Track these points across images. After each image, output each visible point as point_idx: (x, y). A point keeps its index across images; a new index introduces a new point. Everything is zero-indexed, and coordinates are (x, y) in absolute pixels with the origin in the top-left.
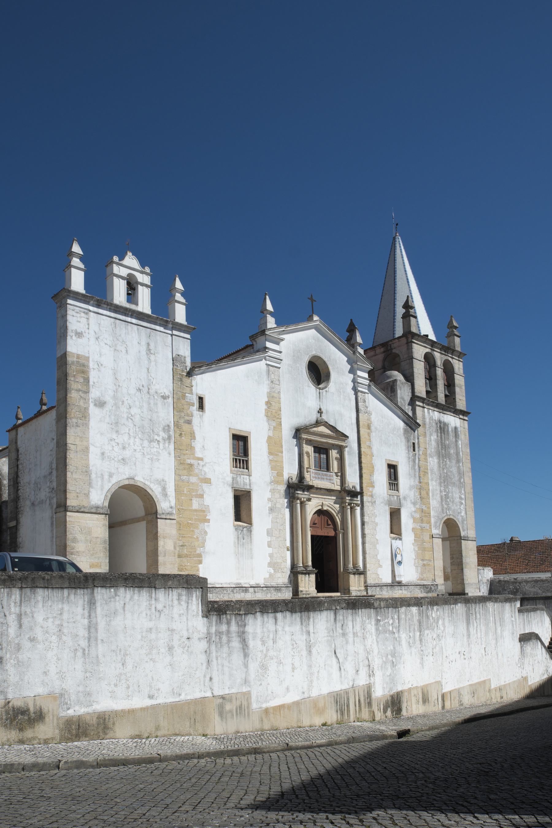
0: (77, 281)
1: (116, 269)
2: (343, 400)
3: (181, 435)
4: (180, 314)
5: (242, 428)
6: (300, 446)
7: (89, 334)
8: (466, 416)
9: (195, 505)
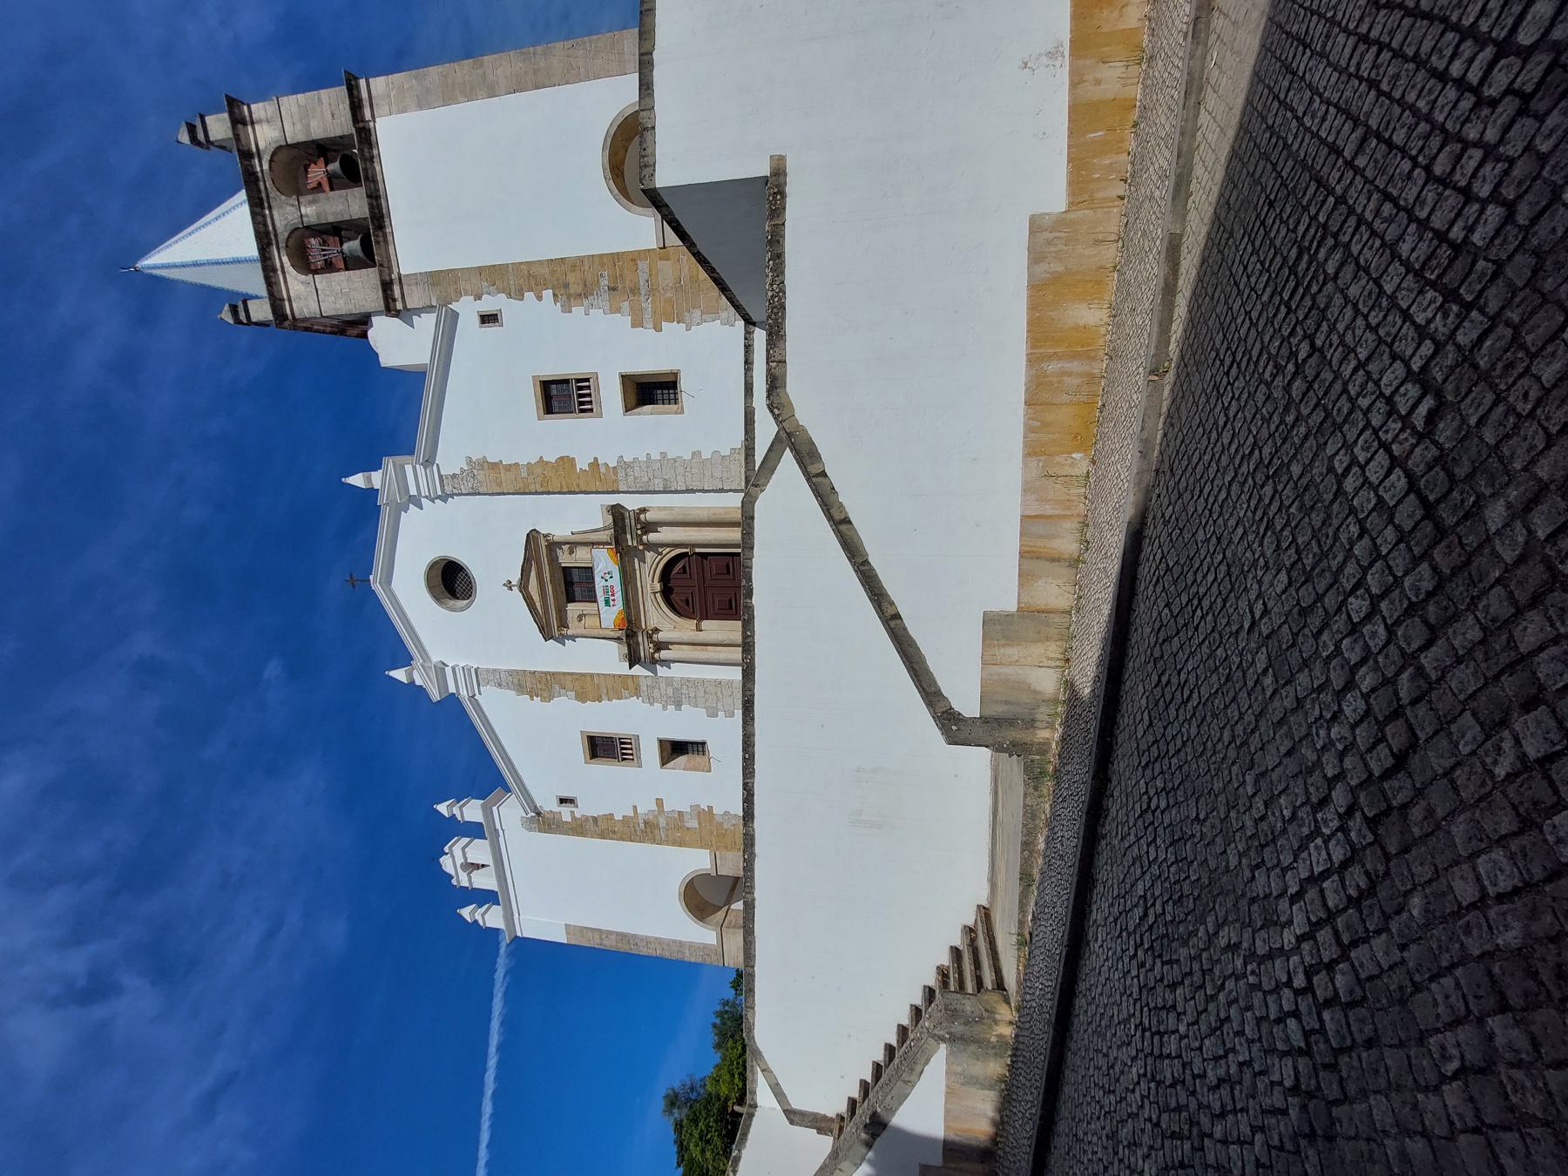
1: (465, 883)
3: (614, 832)
4: (472, 811)
6: (573, 638)
8: (358, 87)
9: (693, 824)
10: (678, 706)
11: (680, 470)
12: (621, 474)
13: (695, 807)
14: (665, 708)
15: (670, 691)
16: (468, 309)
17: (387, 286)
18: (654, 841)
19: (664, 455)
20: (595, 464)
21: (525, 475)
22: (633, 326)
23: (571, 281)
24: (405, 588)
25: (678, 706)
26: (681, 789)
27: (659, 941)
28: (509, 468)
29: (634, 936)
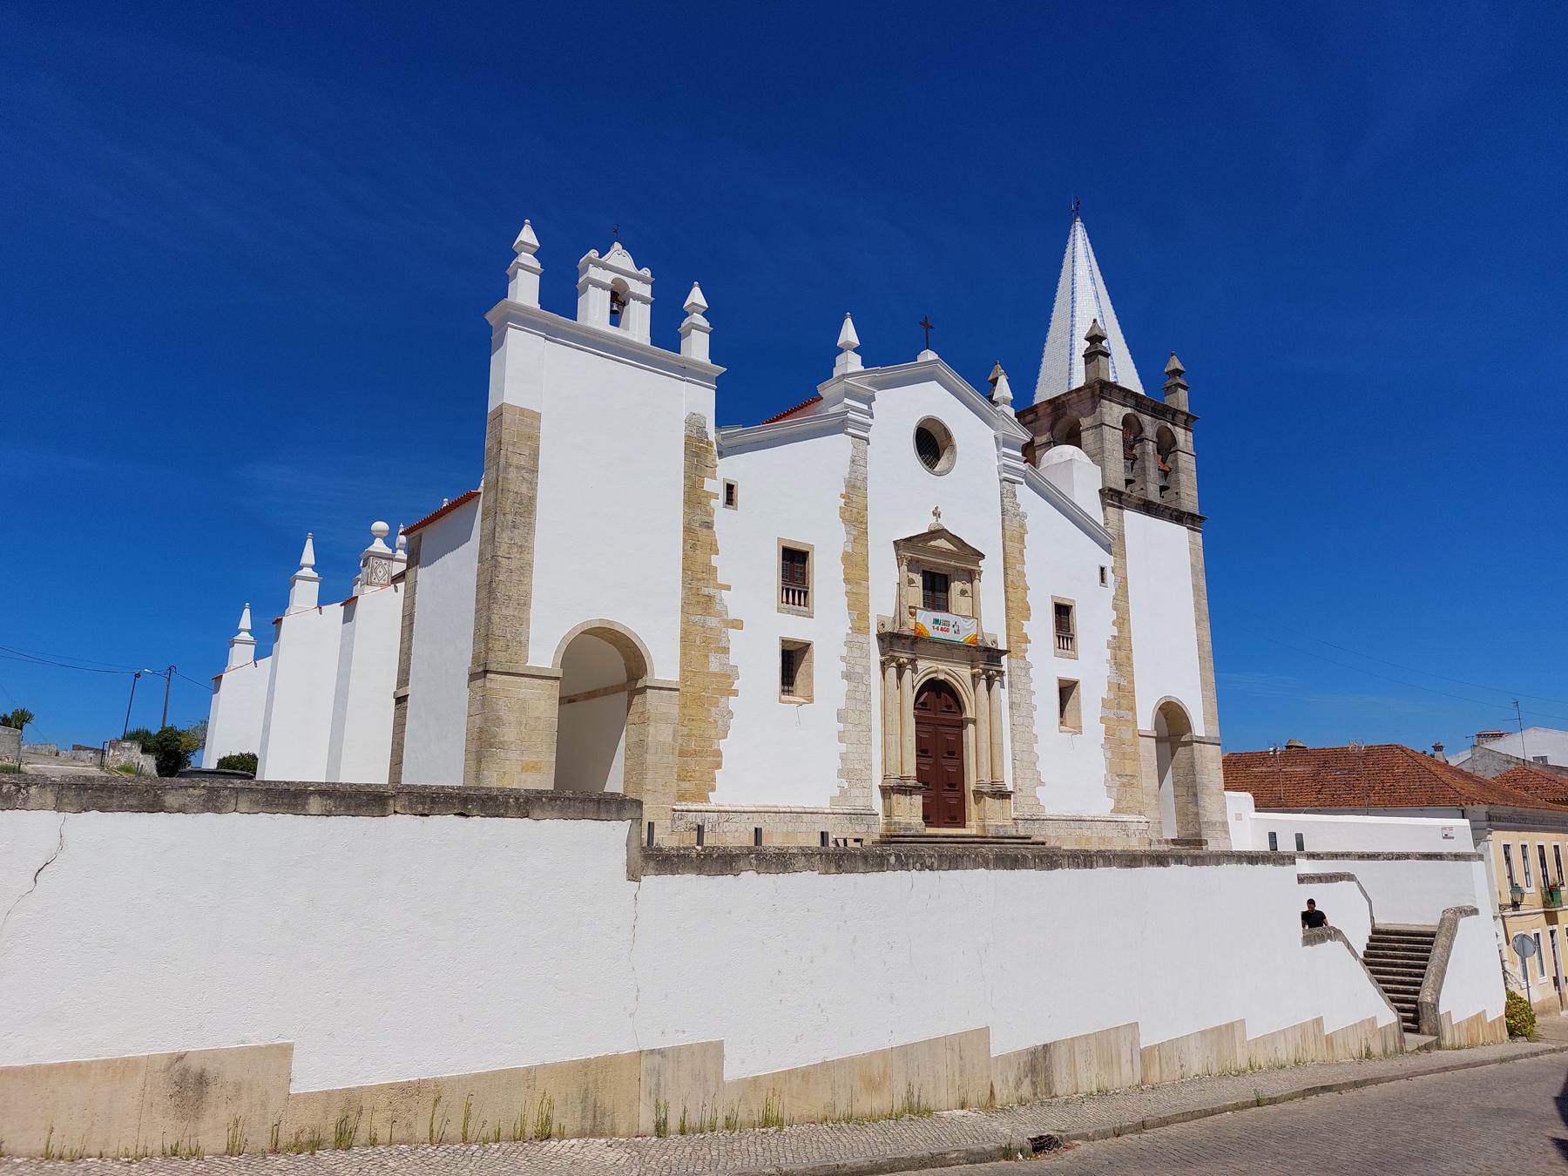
0: (525, 288)
2: (972, 495)
3: (694, 547)
4: (697, 346)
5: (798, 539)
7: (530, 371)
9: (714, 664)
10: (847, 676)
14: (843, 659)
15: (859, 669)
16: (1108, 561)
18: (686, 603)
23: (1121, 650)
24: (933, 397)
27: (526, 568)
29: (530, 527)
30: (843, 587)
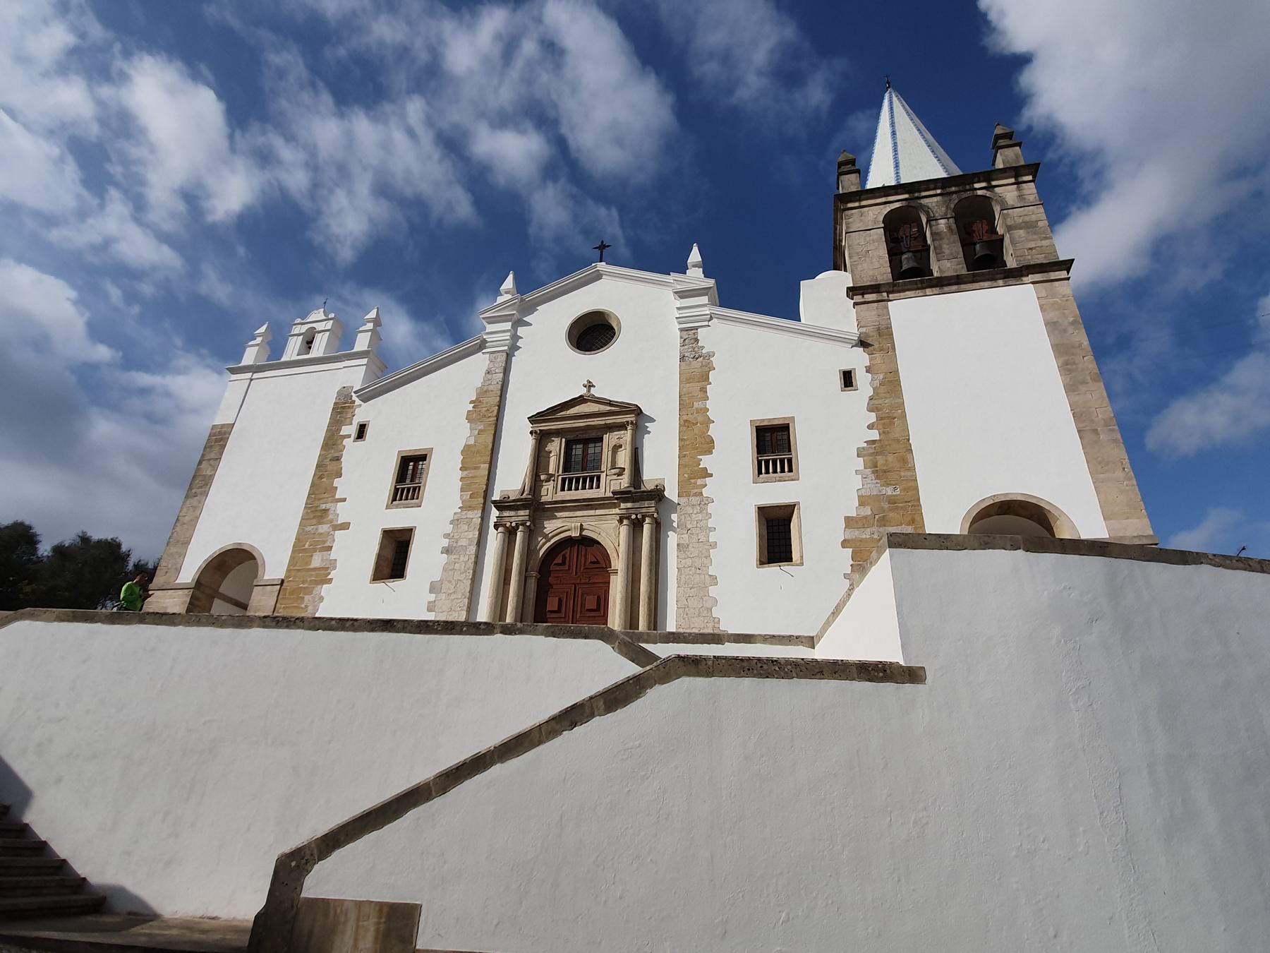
3: (321, 477)
9: (316, 561)
10: (447, 551)
11: (698, 563)
12: (694, 500)
13: (333, 565)
14: (446, 536)
17: (875, 288)
19: (714, 545)
20: (705, 474)
21: (696, 405)
22: (847, 519)
23: (889, 456)
25: (447, 551)
26: (356, 551)
28: (704, 390)
30: (459, 474)
